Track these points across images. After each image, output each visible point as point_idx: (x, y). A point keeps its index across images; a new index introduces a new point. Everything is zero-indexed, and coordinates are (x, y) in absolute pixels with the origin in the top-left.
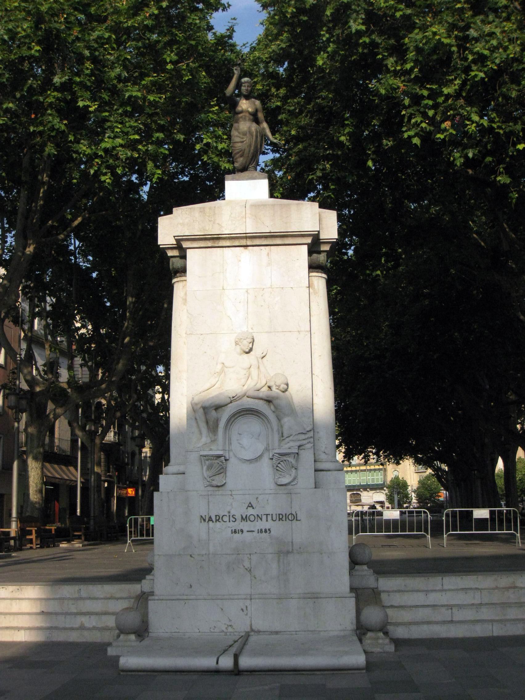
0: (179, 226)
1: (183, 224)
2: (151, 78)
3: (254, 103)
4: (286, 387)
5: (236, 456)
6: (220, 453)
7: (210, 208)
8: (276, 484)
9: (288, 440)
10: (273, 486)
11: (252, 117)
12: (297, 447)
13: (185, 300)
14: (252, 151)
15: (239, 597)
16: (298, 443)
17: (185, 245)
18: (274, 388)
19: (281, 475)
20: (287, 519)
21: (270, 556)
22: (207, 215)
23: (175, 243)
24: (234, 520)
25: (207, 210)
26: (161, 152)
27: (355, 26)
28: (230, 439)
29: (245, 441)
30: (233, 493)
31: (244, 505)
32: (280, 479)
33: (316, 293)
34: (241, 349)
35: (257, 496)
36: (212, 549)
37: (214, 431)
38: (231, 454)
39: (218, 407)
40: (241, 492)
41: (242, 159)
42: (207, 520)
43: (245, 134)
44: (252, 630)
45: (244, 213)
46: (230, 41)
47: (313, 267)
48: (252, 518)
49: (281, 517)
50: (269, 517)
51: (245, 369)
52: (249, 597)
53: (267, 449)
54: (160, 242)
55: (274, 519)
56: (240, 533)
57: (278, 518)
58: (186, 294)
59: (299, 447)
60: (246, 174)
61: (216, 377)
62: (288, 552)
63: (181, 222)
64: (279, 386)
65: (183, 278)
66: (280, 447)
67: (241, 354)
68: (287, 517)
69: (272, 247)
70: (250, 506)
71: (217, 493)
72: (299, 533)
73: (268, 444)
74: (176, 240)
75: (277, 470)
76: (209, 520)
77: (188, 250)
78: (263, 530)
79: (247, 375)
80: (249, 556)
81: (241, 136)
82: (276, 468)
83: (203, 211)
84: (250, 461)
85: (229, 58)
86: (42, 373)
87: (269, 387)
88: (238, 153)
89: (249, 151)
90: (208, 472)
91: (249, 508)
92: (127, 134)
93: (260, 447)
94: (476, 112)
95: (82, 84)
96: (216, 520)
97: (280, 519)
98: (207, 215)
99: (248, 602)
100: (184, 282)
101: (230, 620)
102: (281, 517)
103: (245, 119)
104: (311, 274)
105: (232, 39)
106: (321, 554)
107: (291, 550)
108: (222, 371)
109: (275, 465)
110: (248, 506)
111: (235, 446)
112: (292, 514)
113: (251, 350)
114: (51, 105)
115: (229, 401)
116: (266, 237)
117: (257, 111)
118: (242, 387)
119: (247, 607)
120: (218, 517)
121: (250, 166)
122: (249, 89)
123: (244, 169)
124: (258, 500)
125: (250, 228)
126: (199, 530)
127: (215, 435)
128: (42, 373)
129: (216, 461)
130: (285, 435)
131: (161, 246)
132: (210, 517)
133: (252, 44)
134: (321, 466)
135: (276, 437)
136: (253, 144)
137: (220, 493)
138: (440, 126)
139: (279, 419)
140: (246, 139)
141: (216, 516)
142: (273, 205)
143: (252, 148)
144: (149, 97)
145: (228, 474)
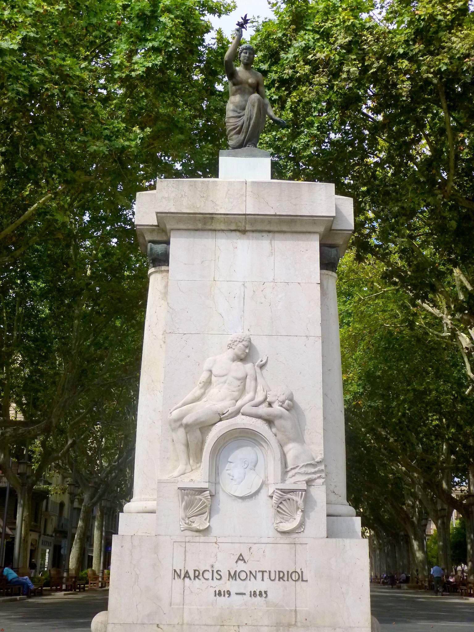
0: (164, 200)
1: (168, 199)
5: (224, 491)
6: (206, 485)
8: (276, 530)
9: (293, 472)
10: (272, 533)
12: (305, 482)
16: (306, 477)
18: (276, 406)
19: (283, 518)
20: (290, 579)
22: (199, 189)
24: (219, 577)
31: (232, 556)
32: (281, 524)
35: (250, 545)
36: (187, 619)
37: (197, 458)
39: (204, 427)
42: (182, 576)
48: (243, 576)
49: (281, 575)
50: (266, 575)
51: (239, 379)
55: (273, 578)
56: (227, 595)
57: (277, 576)
62: (289, 625)
64: (283, 402)
65: (164, 268)
66: (283, 480)
67: (234, 360)
70: (241, 558)
72: (306, 598)
75: (278, 512)
76: (184, 577)
78: (258, 593)
80: (236, 628)
81: (239, 111)
82: (279, 510)
84: (243, 498)
91: (240, 562)
96: (195, 577)
97: (280, 578)
98: (199, 189)
102: (281, 576)
106: (335, 629)
107: (293, 623)
109: (276, 506)
110: (239, 559)
112: (296, 572)
118: (234, 401)
120: (197, 573)
123: (241, 145)
124: (251, 551)
129: (198, 497)
131: (138, 227)
132: (187, 572)
141: (195, 571)
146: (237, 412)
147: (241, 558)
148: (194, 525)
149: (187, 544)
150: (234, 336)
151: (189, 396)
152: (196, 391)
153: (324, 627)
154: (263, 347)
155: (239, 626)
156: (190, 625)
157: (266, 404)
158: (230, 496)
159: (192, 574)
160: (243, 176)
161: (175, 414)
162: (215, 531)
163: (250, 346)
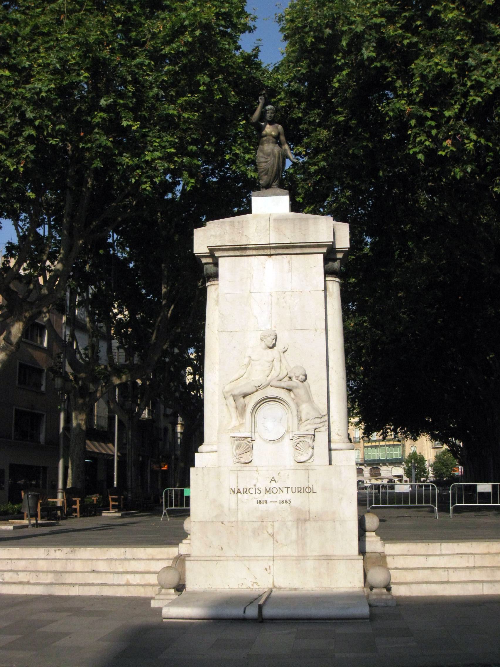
0: (212, 237)
1: (215, 236)
2: (185, 98)
3: (277, 127)
4: (304, 377)
5: (260, 437)
6: (247, 434)
7: (239, 222)
9: (306, 423)
10: (293, 463)
11: (274, 140)
13: (217, 302)
14: (275, 171)
15: (264, 558)
17: (217, 254)
18: (294, 379)
19: (300, 453)
21: (290, 523)
23: (208, 252)
24: (259, 492)
25: (236, 224)
26: (195, 163)
27: (367, 53)
29: (270, 424)
30: (259, 469)
33: (330, 296)
34: (266, 345)
38: (257, 435)
41: (266, 177)
42: (236, 492)
43: (269, 155)
44: (274, 587)
45: (268, 226)
46: (256, 59)
47: (328, 273)
48: (275, 490)
49: (299, 490)
50: (290, 490)
51: (269, 362)
52: (272, 558)
53: (287, 431)
54: (195, 251)
55: (294, 491)
56: (265, 503)
58: (218, 296)
59: (315, 429)
60: (270, 190)
61: (244, 369)
64: (298, 377)
65: (216, 282)
67: (265, 349)
69: (293, 256)
71: (245, 469)
72: (316, 503)
73: (288, 427)
74: (209, 249)
77: (219, 259)
79: (271, 367)
81: (265, 157)
82: (296, 448)
83: (232, 224)
85: (255, 76)
86: (84, 356)
87: (290, 378)
88: (263, 171)
89: (273, 171)
90: (237, 451)
92: (164, 147)
93: (282, 431)
94: (474, 132)
95: (125, 106)
99: (271, 563)
100: (217, 286)
101: (255, 578)
103: (268, 142)
104: (327, 279)
105: (257, 58)
107: (308, 519)
108: (249, 363)
113: (274, 346)
114: (98, 125)
115: (255, 389)
117: (279, 134)
119: (270, 567)
120: (245, 490)
121: (273, 184)
122: (273, 115)
123: (268, 186)
125: (274, 239)
126: (229, 500)
127: (243, 419)
128: (84, 356)
130: (304, 419)
132: (239, 489)
133: (275, 64)
135: (296, 421)
136: (276, 165)
137: (248, 468)
138: (442, 144)
139: (298, 406)
140: (270, 159)
142: (293, 220)
143: (275, 168)
144: (184, 115)
148: (243, 460)
149: (238, 472)
151: (237, 376)
153: (328, 520)
155: (273, 522)
156: (243, 522)
157: (287, 379)
158: (264, 440)
159: (242, 491)
160: (270, 207)
161: (227, 388)
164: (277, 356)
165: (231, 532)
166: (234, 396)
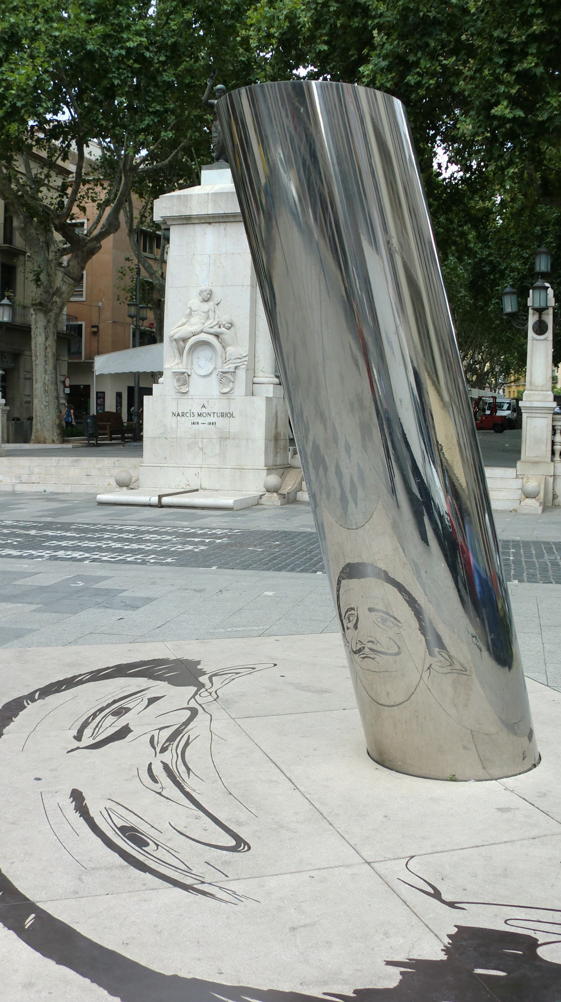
1: (166, 208)
9: (228, 362)
10: (218, 394)
28: (192, 362)
29: (202, 362)
36: (179, 435)
39: (185, 340)
40: (198, 397)
48: (204, 415)
50: (215, 415)
51: (204, 312)
53: (215, 369)
62: (226, 438)
63: (164, 206)
66: (222, 367)
67: (202, 302)
68: (227, 415)
70: (204, 406)
71: (183, 397)
79: (206, 317)
93: (211, 367)
111: (195, 366)
116: (223, 217)
132: (178, 414)
134: (256, 380)
135: (220, 361)
145: (190, 384)
146: (202, 331)
147: (204, 406)
148: (181, 391)
150: (203, 287)
152: (184, 320)
154: (218, 294)
156: (180, 438)
162: (191, 393)
163: (211, 293)
164: (213, 308)
165: (172, 446)
166: (175, 340)
